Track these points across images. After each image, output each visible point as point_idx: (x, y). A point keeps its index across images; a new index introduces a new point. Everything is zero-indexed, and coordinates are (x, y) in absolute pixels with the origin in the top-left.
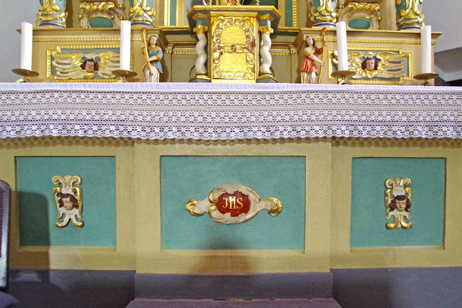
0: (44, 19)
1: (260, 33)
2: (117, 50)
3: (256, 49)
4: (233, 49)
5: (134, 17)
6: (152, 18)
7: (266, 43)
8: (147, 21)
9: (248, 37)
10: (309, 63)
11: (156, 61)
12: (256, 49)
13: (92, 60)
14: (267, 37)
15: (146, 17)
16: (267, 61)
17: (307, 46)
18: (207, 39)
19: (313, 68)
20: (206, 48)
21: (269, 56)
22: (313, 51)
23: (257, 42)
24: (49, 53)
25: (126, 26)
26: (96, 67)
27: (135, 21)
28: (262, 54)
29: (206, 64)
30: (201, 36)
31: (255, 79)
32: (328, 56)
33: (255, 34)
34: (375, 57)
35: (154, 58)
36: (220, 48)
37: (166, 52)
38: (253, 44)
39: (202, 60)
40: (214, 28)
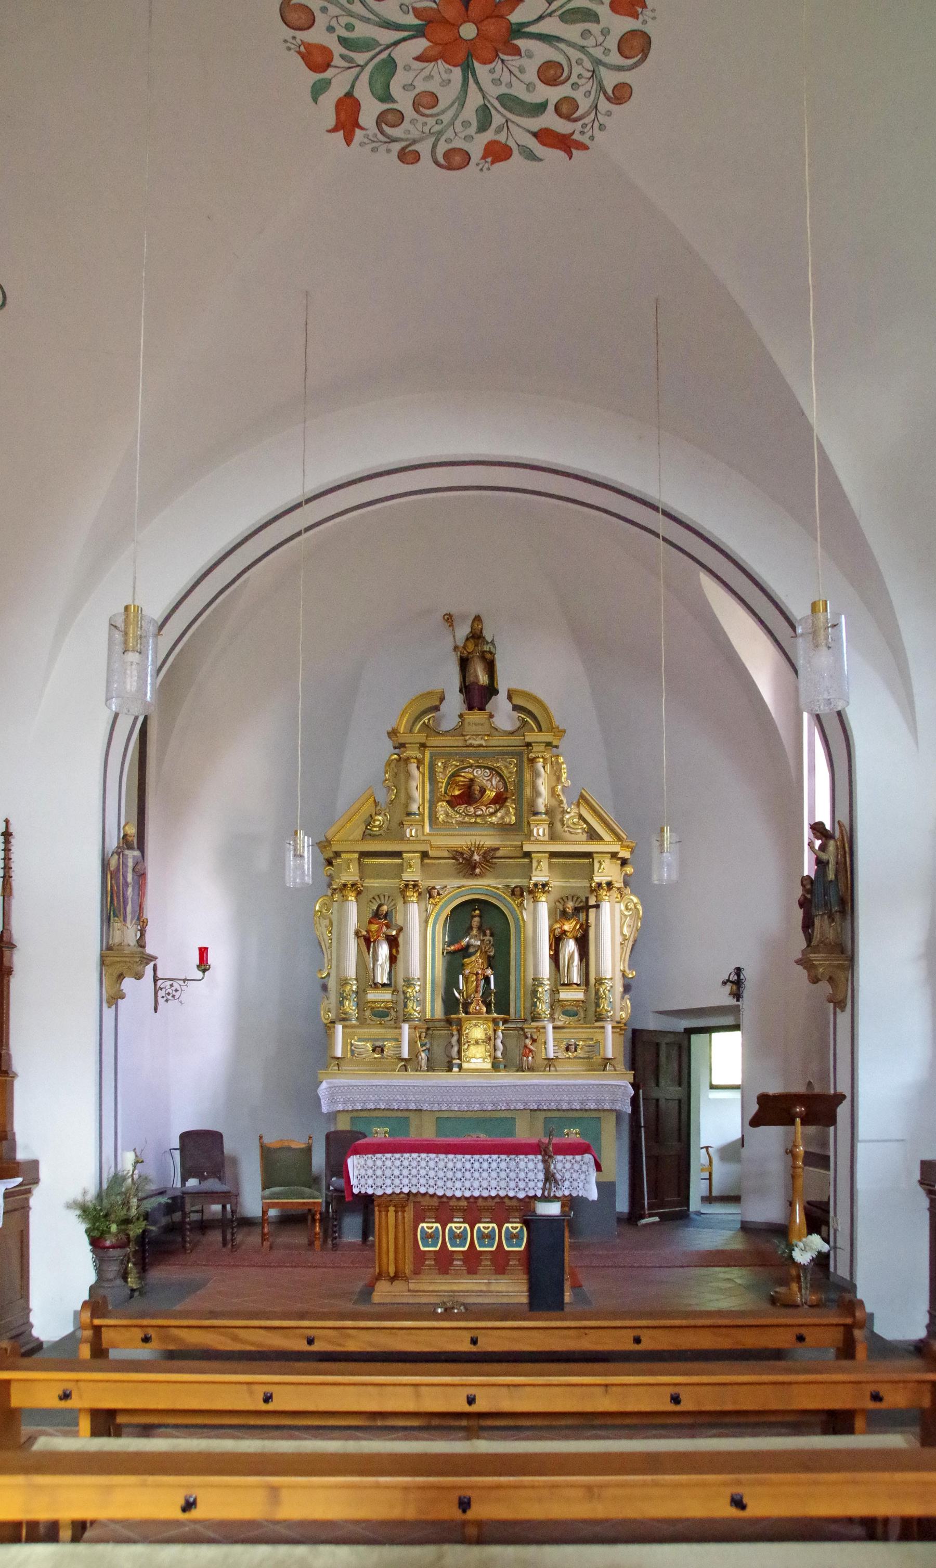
0: (344, 1016)
1: (495, 1031)
2: (398, 1040)
3: (492, 1043)
4: (477, 1043)
7: (499, 1037)
9: (486, 1034)
10: (527, 1051)
12: (492, 1043)
13: (380, 1047)
14: (500, 1033)
17: (527, 1038)
20: (459, 1041)
23: (492, 1038)
24: (349, 1041)
25: (406, 1027)
26: (382, 1051)
29: (459, 1052)
30: (455, 1033)
33: (491, 1032)
34: (575, 1043)
35: (424, 1048)
36: (468, 1042)
38: (490, 1039)
39: (456, 1049)
40: (464, 1028)
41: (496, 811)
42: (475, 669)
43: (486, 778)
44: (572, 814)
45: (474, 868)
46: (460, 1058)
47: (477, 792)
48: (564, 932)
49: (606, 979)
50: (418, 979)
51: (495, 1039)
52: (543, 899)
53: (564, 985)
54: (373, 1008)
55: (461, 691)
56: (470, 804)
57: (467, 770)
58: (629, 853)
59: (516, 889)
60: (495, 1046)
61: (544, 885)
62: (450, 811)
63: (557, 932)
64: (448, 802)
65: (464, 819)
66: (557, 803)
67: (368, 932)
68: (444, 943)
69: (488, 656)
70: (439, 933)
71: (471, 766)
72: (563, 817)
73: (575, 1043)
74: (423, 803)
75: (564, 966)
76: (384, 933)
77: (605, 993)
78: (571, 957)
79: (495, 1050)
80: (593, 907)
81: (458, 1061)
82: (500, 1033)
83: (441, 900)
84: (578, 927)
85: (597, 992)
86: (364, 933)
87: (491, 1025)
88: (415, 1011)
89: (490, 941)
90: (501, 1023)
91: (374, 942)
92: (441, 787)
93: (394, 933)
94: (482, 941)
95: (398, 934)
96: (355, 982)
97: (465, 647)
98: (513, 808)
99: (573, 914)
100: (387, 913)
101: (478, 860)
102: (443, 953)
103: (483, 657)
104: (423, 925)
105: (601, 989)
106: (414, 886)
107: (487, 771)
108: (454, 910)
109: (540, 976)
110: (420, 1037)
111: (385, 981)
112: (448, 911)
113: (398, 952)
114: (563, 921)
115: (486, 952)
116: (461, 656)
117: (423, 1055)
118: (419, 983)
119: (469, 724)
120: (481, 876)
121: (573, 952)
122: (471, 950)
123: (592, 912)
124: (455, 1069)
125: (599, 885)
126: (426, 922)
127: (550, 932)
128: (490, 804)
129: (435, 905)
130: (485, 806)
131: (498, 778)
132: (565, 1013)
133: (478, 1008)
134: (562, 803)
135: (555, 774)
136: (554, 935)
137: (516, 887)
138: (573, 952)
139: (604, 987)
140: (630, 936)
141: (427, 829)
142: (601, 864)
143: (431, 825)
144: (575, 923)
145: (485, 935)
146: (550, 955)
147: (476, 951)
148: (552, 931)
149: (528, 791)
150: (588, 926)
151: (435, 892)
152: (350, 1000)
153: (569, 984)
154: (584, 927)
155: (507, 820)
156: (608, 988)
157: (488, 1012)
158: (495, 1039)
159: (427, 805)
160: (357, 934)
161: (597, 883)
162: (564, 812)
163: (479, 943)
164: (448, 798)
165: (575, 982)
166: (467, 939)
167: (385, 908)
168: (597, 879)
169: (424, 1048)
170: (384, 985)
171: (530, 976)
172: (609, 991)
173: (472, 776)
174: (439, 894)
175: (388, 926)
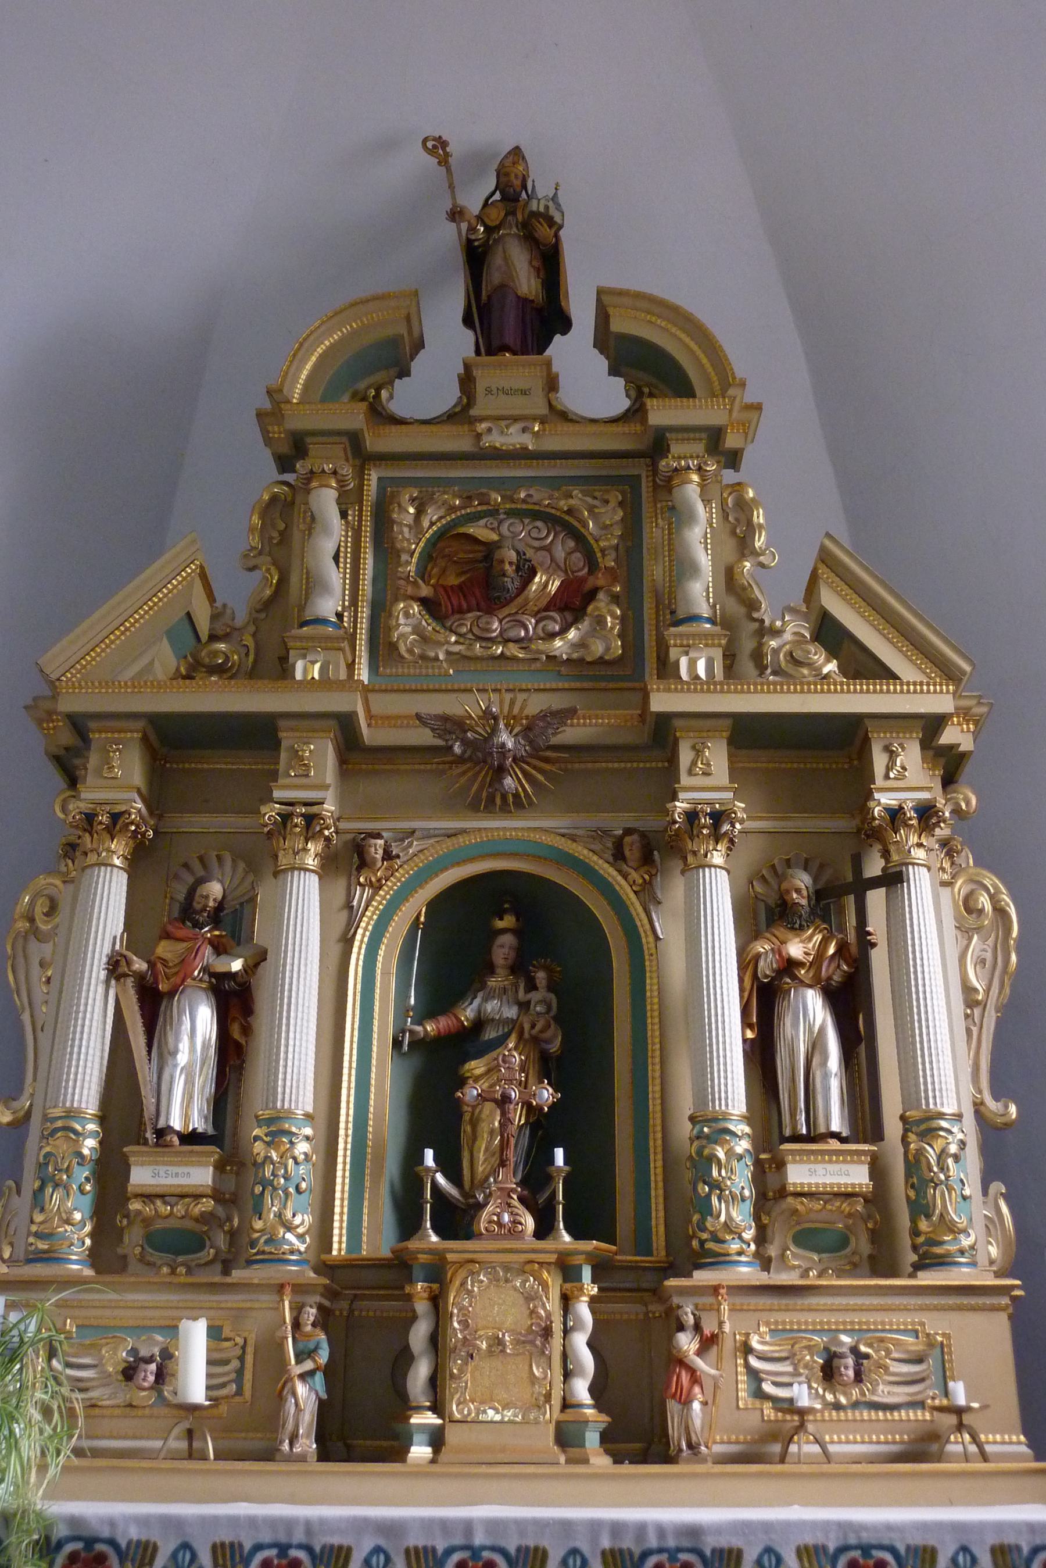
1: (566, 1301)
5: (262, 1240)
6: (304, 1242)
7: (579, 1326)
8: (292, 1252)
10: (685, 1378)
11: (311, 1373)
15: (291, 1244)
16: (582, 1373)
17: (681, 1328)
18: (437, 1355)
19: (697, 1389)
20: (435, 1341)
21: (587, 1359)
22: (694, 1346)
23: (557, 1327)
27: (263, 1252)
28: (569, 1352)
29: (434, 1382)
30: (422, 1306)
31: (554, 1422)
32: (736, 1349)
33: (553, 1304)
35: (309, 1365)
37: (334, 1314)
41: (564, 630)
42: (506, 259)
43: (536, 544)
44: (788, 636)
45: (500, 771)
46: (437, 1408)
47: (509, 569)
48: (790, 966)
49: (941, 1116)
50: (308, 1116)
51: (566, 1332)
52: (717, 858)
53: (797, 1138)
54: (147, 1222)
55: (468, 321)
56: (490, 611)
57: (482, 522)
58: (970, 737)
59: (628, 839)
60: (565, 1356)
61: (718, 817)
62: (429, 625)
63: (766, 967)
64: (424, 602)
65: (470, 646)
66: (742, 610)
67: (152, 965)
68: (402, 1010)
69: (544, 232)
70: (385, 973)
71: (493, 513)
72: (760, 645)
73: (854, 1350)
74: (354, 602)
75: (793, 1080)
76: (205, 969)
77: (944, 1168)
78: (817, 1044)
79: (567, 1375)
80: (876, 883)
81: (430, 1419)
82: (583, 1310)
83: (392, 872)
84: (831, 950)
85: (914, 1164)
86: (140, 965)
87: (554, 1282)
88: (290, 1228)
89: (549, 1009)
90: (587, 1273)
91: (172, 994)
92: (409, 563)
93: (237, 965)
94: (524, 1006)
95: (251, 968)
96: (92, 1127)
97: (479, 218)
98: (614, 616)
99: (813, 912)
100: (220, 906)
101: (510, 745)
102: (397, 1043)
103: (530, 238)
104: (336, 949)
105: (932, 1155)
106: (310, 819)
107: (539, 524)
108: (433, 905)
109: (720, 1107)
110: (297, 1325)
111: (198, 1123)
112: (417, 904)
113: (247, 1030)
114: (780, 932)
115: (535, 1040)
116: (469, 242)
117: (301, 1389)
118: (308, 1131)
119: (489, 391)
120: (518, 804)
121: (822, 1029)
122: (490, 1034)
123: (876, 899)
124: (420, 1451)
125: (895, 815)
126: (347, 941)
127: (742, 968)
128: (547, 609)
129: (377, 887)
130: (534, 616)
131: (571, 544)
132: (806, 1239)
133: (506, 1218)
134: (758, 609)
135: (733, 533)
136: (755, 976)
137: (628, 832)
138: (822, 1029)
139: (939, 1144)
140: (987, 991)
141: (363, 674)
142: (892, 754)
143: (374, 667)
144: (818, 938)
145: (532, 986)
146: (745, 1040)
147: (506, 1037)
148: (746, 963)
149: (655, 571)
150: (866, 943)
151: (376, 848)
152: (67, 1188)
153: (811, 1138)
154: (854, 950)
155: (598, 648)
156: (953, 1149)
157: (544, 1230)
158: (566, 1332)
159: (364, 613)
160: (115, 968)
161: (888, 809)
162: (764, 632)
163: (511, 1012)
164: (425, 591)
165: (835, 1127)
166: (477, 1002)
167: (215, 889)
168: (884, 799)
169: (309, 1365)
170: (191, 1138)
171: (685, 1104)
172: (956, 1158)
173: (495, 537)
174: (388, 856)
175: (220, 949)
